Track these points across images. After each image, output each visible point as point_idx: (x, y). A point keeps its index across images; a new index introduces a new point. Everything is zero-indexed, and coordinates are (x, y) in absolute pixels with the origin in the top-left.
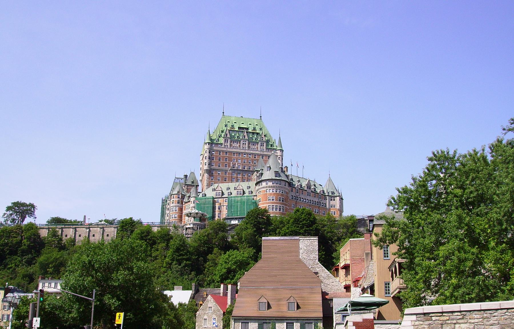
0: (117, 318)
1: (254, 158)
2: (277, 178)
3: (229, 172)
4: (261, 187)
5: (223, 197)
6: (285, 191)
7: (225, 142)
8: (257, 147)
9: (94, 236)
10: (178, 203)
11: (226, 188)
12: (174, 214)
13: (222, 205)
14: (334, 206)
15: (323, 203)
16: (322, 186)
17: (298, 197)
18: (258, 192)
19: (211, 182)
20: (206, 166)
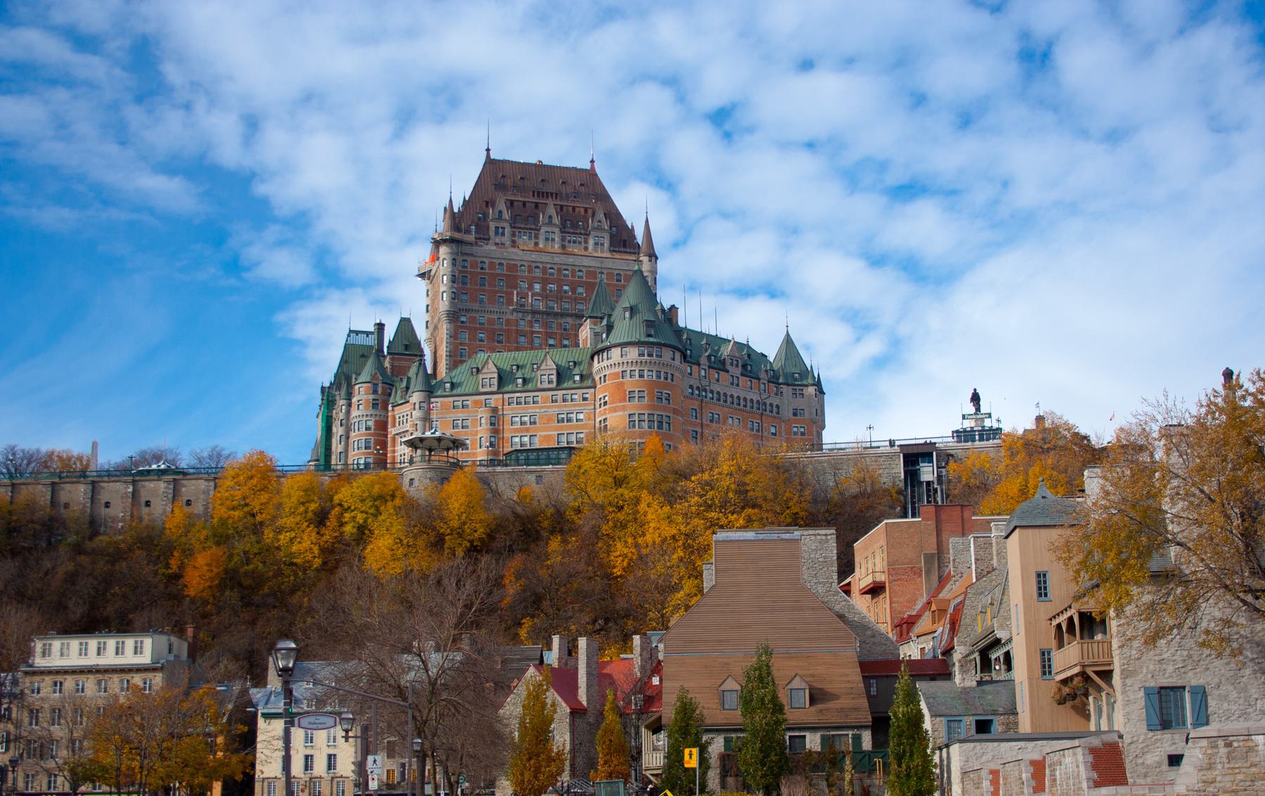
0: (687, 757)
2: (651, 340)
4: (606, 363)
6: (672, 375)
9: (148, 504)
10: (375, 406)
12: (364, 438)
14: (800, 414)
15: (771, 405)
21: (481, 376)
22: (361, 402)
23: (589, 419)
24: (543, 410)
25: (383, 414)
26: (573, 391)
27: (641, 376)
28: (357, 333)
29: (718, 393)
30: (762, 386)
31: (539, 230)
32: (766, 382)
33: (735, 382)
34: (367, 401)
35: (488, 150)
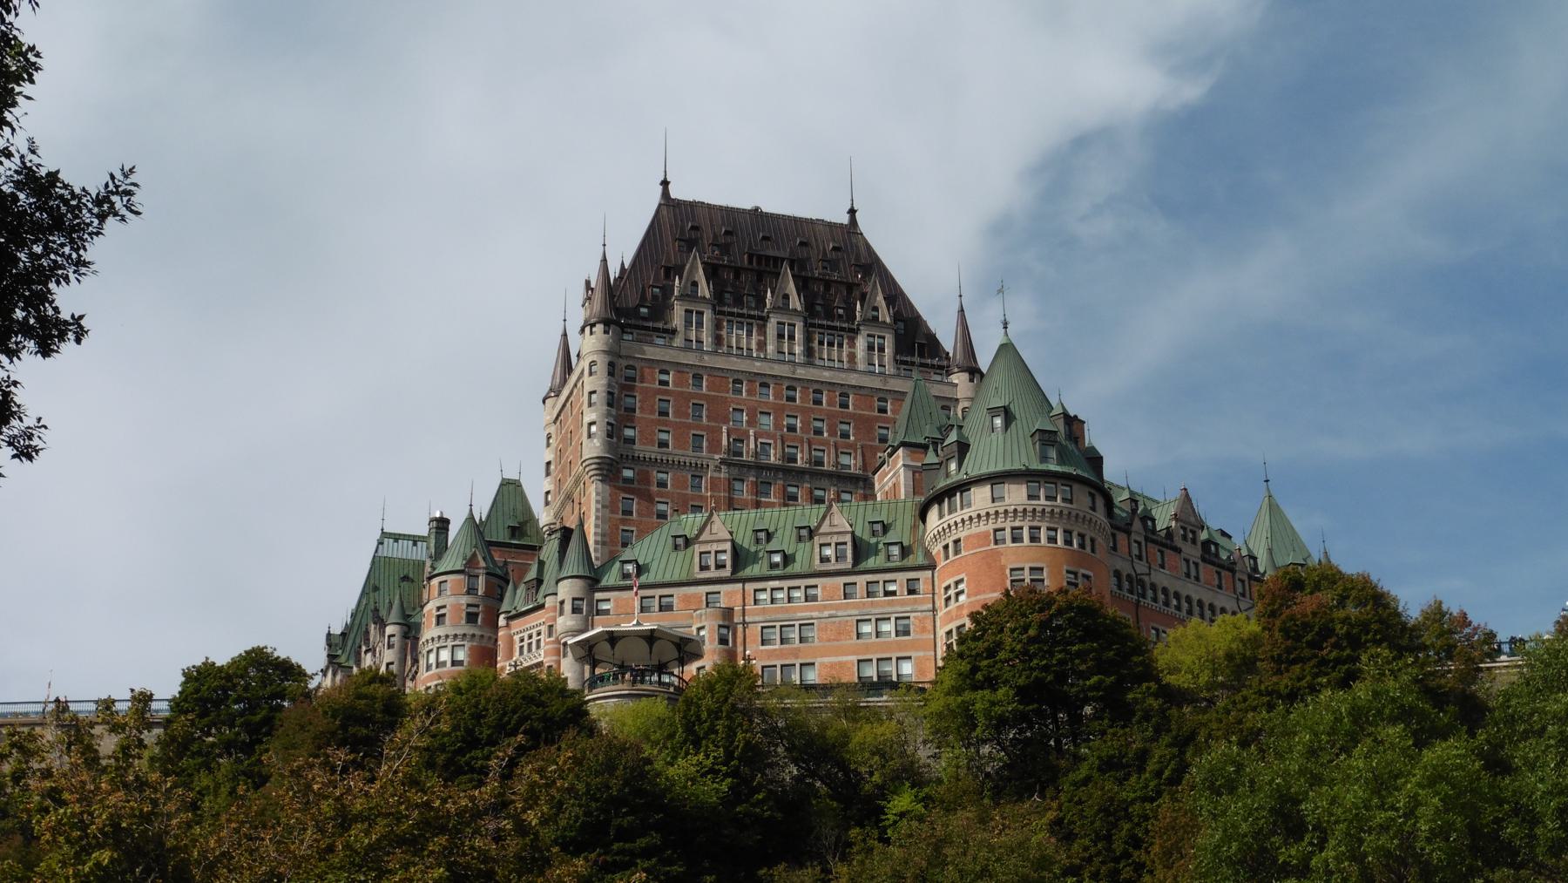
1: (841, 406)
2: (1053, 467)
3: (716, 475)
4: (957, 517)
5: (741, 574)
6: (1093, 541)
7: (688, 323)
8: (852, 357)
10: (471, 618)
11: (749, 532)
13: (736, 620)
16: (1230, 537)
17: (1141, 583)
18: (946, 547)
19: (622, 527)
20: (595, 441)
21: (698, 548)
22: (442, 611)
23: (924, 630)
24: (826, 614)
25: (487, 635)
26: (888, 576)
27: (1034, 539)
28: (397, 538)
29: (1165, 591)
30: (1239, 585)
31: (765, 319)
32: (1245, 578)
33: (1193, 573)
34: (457, 607)
35: (665, 183)
